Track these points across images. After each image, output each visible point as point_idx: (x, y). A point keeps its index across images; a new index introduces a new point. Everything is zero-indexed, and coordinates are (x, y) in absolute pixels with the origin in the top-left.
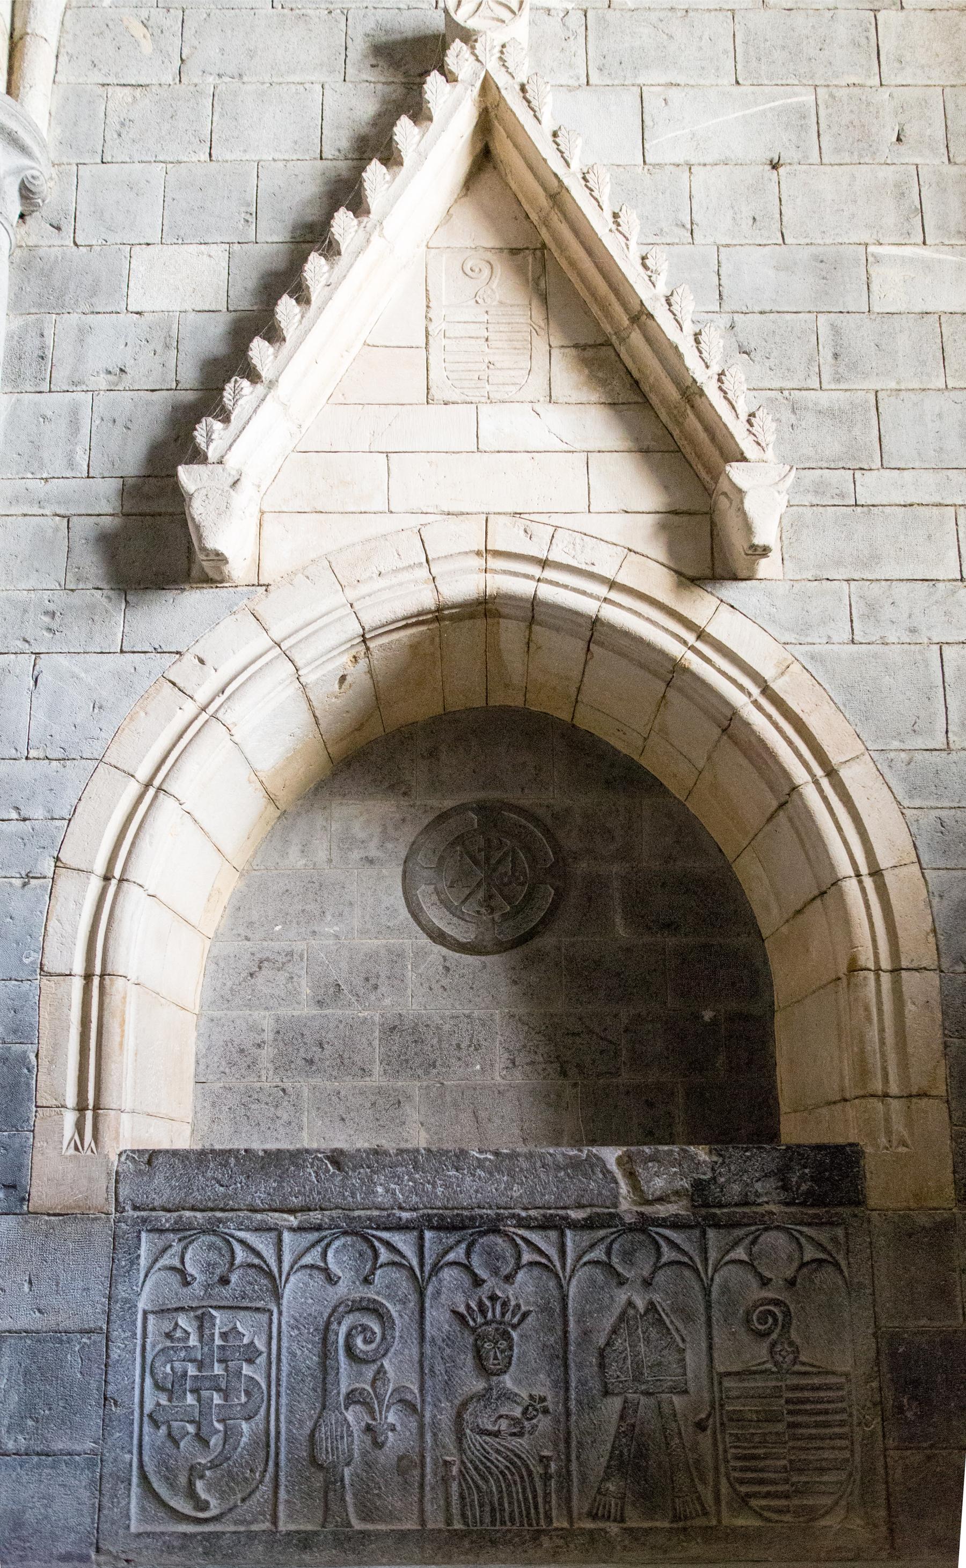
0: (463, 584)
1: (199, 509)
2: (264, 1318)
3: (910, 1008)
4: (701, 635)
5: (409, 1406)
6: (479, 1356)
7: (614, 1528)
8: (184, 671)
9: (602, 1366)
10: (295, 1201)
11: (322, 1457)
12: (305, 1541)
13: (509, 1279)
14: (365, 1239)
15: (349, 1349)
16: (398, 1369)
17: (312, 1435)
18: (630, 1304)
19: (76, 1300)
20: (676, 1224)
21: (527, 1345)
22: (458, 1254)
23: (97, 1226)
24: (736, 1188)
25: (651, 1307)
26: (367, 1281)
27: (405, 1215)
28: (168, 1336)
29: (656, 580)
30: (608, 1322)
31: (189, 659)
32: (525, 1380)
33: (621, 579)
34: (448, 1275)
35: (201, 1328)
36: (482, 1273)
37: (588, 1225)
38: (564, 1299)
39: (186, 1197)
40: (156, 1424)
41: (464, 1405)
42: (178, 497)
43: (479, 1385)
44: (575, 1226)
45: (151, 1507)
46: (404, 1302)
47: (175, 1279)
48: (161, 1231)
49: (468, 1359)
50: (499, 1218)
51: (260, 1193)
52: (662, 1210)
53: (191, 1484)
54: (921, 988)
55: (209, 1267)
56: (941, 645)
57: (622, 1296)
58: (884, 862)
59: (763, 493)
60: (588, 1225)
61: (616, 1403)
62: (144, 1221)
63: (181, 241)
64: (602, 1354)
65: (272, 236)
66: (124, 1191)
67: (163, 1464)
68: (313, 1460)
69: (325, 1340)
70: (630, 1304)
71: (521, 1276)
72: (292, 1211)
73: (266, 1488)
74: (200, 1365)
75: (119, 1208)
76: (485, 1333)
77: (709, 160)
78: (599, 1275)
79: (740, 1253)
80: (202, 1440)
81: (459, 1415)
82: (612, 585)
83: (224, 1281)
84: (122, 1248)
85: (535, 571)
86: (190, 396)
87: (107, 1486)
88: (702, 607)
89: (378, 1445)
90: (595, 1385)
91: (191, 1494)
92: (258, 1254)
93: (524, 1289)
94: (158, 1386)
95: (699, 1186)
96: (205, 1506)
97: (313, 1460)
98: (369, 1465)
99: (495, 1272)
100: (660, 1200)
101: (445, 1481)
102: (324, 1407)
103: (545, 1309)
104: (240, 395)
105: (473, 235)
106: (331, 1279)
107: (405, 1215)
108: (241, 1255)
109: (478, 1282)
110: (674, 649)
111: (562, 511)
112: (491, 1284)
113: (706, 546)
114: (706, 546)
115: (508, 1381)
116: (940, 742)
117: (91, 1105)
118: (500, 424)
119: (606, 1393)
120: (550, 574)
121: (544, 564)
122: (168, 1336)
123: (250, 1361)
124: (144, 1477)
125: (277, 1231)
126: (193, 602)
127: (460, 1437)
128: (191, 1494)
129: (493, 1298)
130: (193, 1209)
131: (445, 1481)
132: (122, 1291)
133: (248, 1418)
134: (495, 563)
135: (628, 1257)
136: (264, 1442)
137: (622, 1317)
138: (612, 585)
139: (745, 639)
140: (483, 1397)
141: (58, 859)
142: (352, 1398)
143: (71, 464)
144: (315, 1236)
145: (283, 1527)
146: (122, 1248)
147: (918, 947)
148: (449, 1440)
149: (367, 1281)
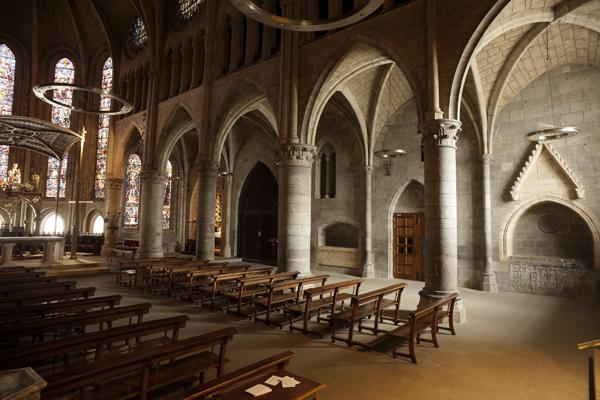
16: (538, 278)
19: (505, 268)
29: (568, 199)
39: (514, 261)
42: (511, 195)
59: (581, 193)
65: (518, 161)
76: (548, 277)
84: (509, 265)
88: (574, 202)
104: (516, 183)
105: (542, 159)
111: (555, 192)
114: (574, 196)
117: (505, 252)
118: (546, 181)
126: (512, 203)
139: (578, 207)
146: (509, 265)
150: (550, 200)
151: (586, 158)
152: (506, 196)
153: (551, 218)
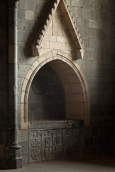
0: (55, 58)
1: (39, 51)
2: (40, 139)
3: (88, 106)
4: (74, 65)
5: (52, 147)
6: (57, 142)
7: (66, 157)
8: (32, 67)
9: (65, 142)
10: (43, 127)
11: (45, 153)
12: (44, 161)
13: (59, 134)
14: (48, 131)
15: (47, 142)
16: (51, 145)
17: (44, 151)
18: (68, 136)
20: (71, 128)
21: (60, 140)
22: (55, 132)
23: (27, 131)
24: (75, 124)
25: (69, 136)
26: (48, 135)
27: (51, 128)
28: (33, 142)
30: (66, 138)
31: (32, 66)
32: (60, 144)
33: (68, 59)
34: (54, 134)
35: (35, 141)
36: (57, 134)
37: (65, 129)
38: (63, 136)
40: (32, 151)
41: (56, 147)
43: (57, 145)
44: (64, 129)
45: (32, 159)
46: (51, 137)
47: (33, 136)
48: (32, 131)
49: (56, 142)
50: (58, 128)
51: (40, 127)
52: (70, 127)
53: (35, 156)
54: (89, 104)
55: (36, 134)
56: (92, 68)
57: (67, 135)
58: (87, 91)
60: (65, 129)
61: (66, 145)
62: (31, 130)
63: (30, 10)
64: (65, 141)
66: (29, 127)
67: (33, 155)
68: (44, 153)
69: (45, 141)
70: (68, 136)
71: (60, 134)
72: (42, 128)
73: (41, 156)
74: (36, 145)
75: (29, 129)
77: (76, 6)
78: (65, 133)
79: (75, 131)
80: (36, 152)
81: (55, 148)
82: (67, 59)
83: (37, 136)
85: (61, 57)
86: (32, 32)
87: (29, 157)
89: (49, 151)
90: (65, 144)
91: (35, 157)
92: (40, 133)
93: (60, 135)
94: (32, 147)
95: (73, 124)
96: (36, 158)
97: (44, 153)
98: (49, 153)
99: (58, 134)
100: (70, 126)
101: (54, 154)
102: (45, 148)
103: (61, 137)
106: (45, 135)
107: (51, 128)
108: (39, 133)
109: (57, 135)
110: (72, 67)
112: (58, 135)
113: (75, 54)
115: (59, 144)
116: (91, 79)
119: (66, 145)
120: (62, 57)
121: (62, 56)
122: (33, 142)
123: (39, 144)
124: (32, 156)
125: (41, 131)
127: (55, 149)
128: (35, 157)
129: (58, 136)
130: (35, 129)
131: (54, 154)
132: (29, 138)
133: (40, 149)
134: (58, 56)
135: (68, 132)
136: (41, 151)
137: (67, 138)
138: (67, 59)
139: (77, 66)
140: (57, 146)
141: (21, 90)
142: (47, 147)
143: (20, 40)
144: (44, 131)
145: (43, 160)
147: (89, 100)
148: (55, 150)
149: (48, 135)
150: (60, 59)
151: (82, 21)
152: (30, 51)
153: (51, 76)
